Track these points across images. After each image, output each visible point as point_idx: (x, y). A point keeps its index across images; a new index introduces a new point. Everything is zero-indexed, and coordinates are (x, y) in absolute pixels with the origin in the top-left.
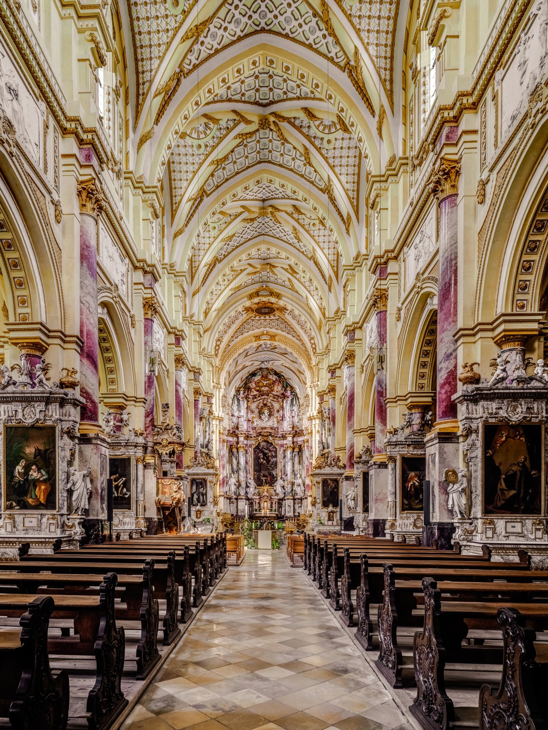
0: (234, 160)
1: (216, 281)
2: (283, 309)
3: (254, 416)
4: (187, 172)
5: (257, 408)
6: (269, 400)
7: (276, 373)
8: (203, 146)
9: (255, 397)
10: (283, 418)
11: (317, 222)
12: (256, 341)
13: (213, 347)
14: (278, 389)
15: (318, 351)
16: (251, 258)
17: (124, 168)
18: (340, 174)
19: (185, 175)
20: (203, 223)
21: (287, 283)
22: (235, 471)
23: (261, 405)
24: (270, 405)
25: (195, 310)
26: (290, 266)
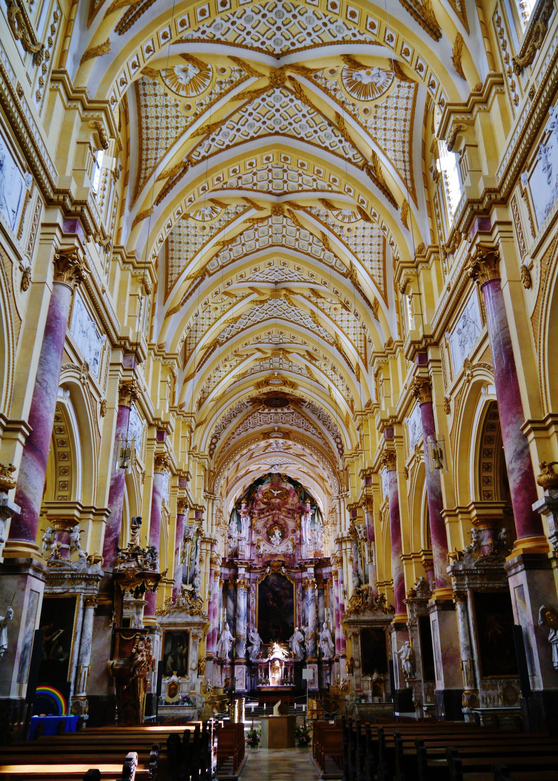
0: (243, 242)
1: (217, 366)
2: (299, 402)
3: (260, 538)
4: (188, 251)
5: (265, 526)
6: (282, 517)
7: (290, 480)
8: (208, 229)
9: (261, 511)
10: (300, 541)
11: (339, 306)
12: (264, 439)
13: (207, 445)
14: (293, 501)
15: (346, 452)
16: (260, 342)
17: (113, 242)
18: (364, 260)
19: (185, 254)
20: (203, 302)
21: (305, 371)
22: (232, 621)
23: (271, 522)
24: (282, 522)
25: (187, 399)
26: (307, 351)
